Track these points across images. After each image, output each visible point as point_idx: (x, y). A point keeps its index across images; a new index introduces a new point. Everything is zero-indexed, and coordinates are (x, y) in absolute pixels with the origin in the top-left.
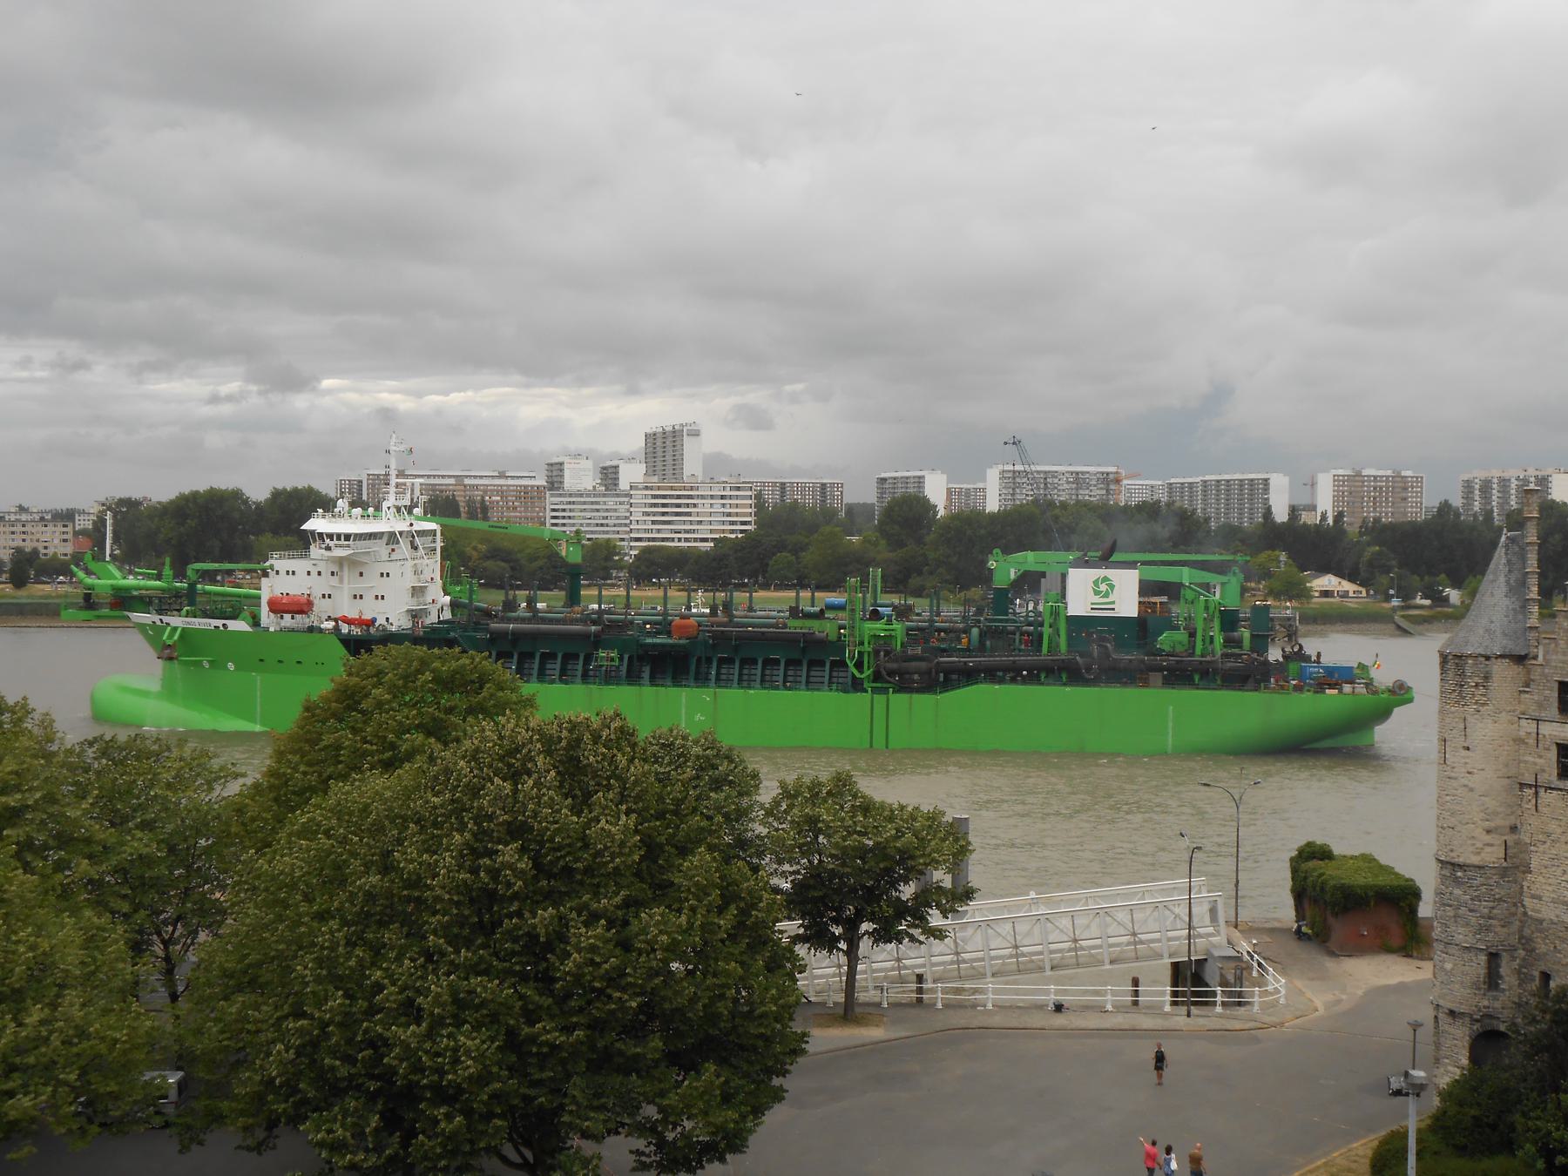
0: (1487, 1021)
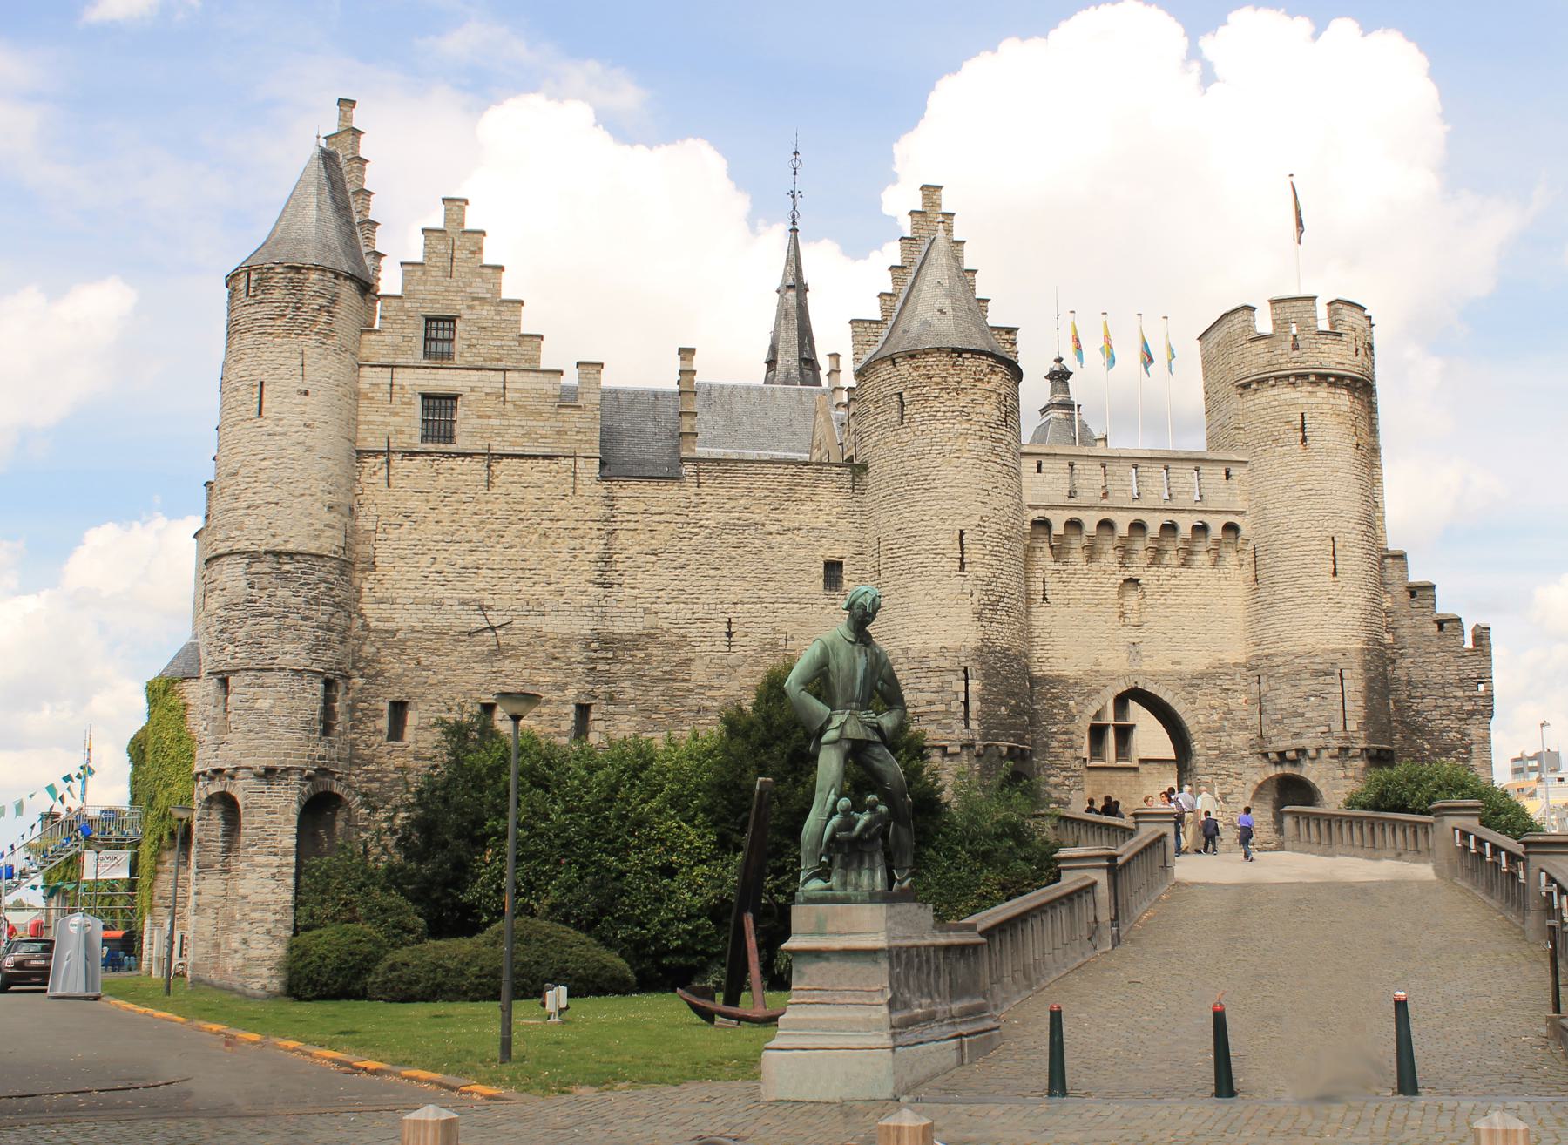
0: (320, 779)
